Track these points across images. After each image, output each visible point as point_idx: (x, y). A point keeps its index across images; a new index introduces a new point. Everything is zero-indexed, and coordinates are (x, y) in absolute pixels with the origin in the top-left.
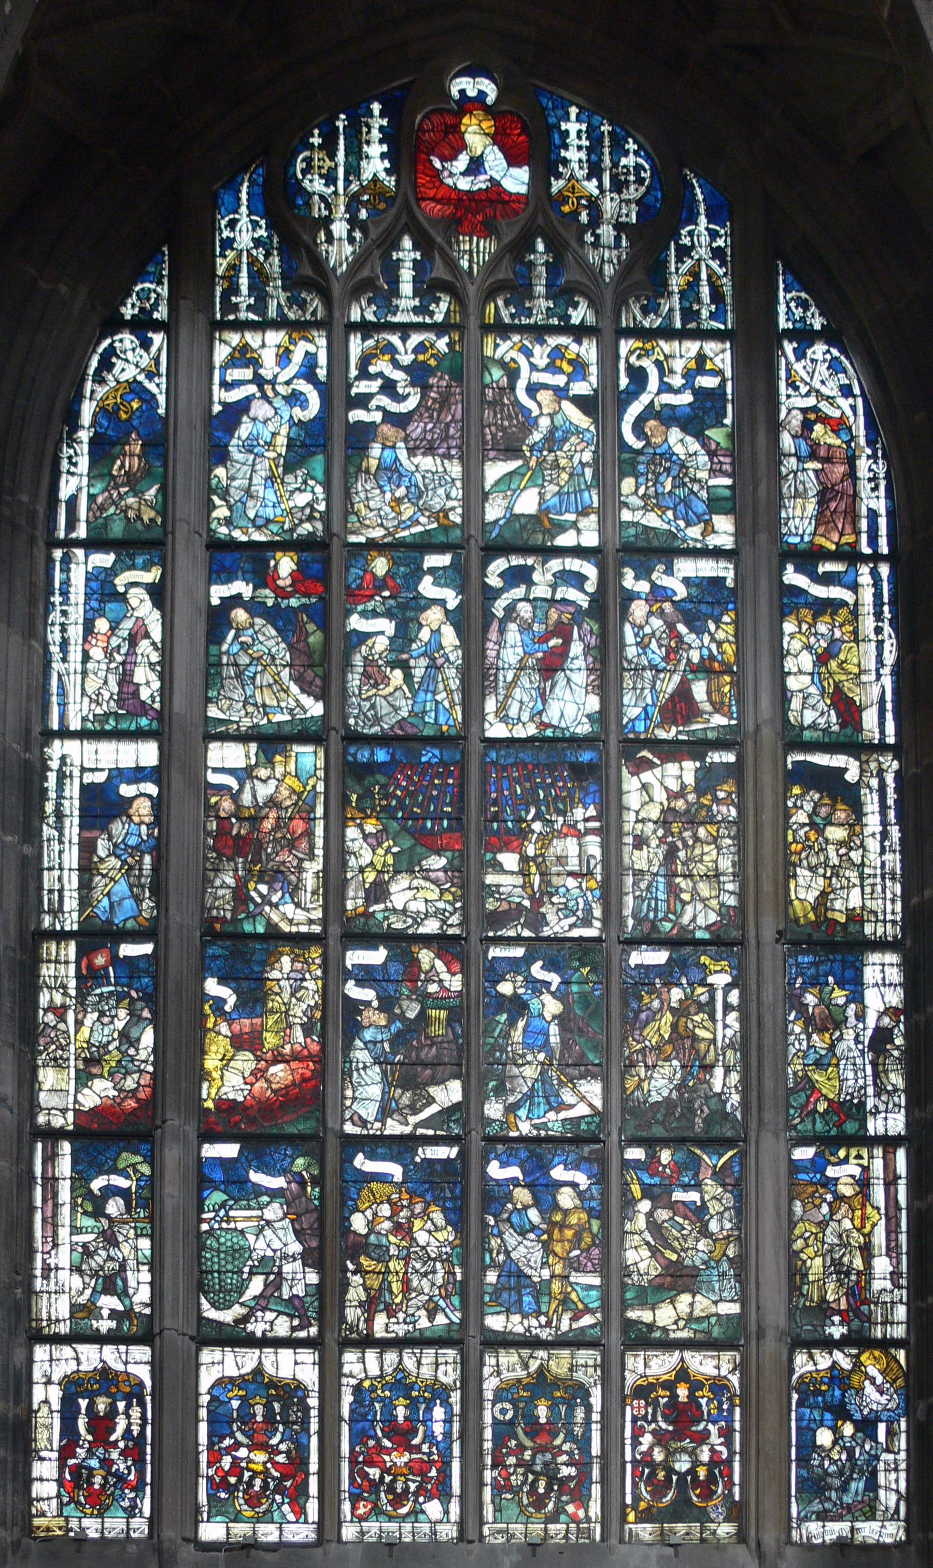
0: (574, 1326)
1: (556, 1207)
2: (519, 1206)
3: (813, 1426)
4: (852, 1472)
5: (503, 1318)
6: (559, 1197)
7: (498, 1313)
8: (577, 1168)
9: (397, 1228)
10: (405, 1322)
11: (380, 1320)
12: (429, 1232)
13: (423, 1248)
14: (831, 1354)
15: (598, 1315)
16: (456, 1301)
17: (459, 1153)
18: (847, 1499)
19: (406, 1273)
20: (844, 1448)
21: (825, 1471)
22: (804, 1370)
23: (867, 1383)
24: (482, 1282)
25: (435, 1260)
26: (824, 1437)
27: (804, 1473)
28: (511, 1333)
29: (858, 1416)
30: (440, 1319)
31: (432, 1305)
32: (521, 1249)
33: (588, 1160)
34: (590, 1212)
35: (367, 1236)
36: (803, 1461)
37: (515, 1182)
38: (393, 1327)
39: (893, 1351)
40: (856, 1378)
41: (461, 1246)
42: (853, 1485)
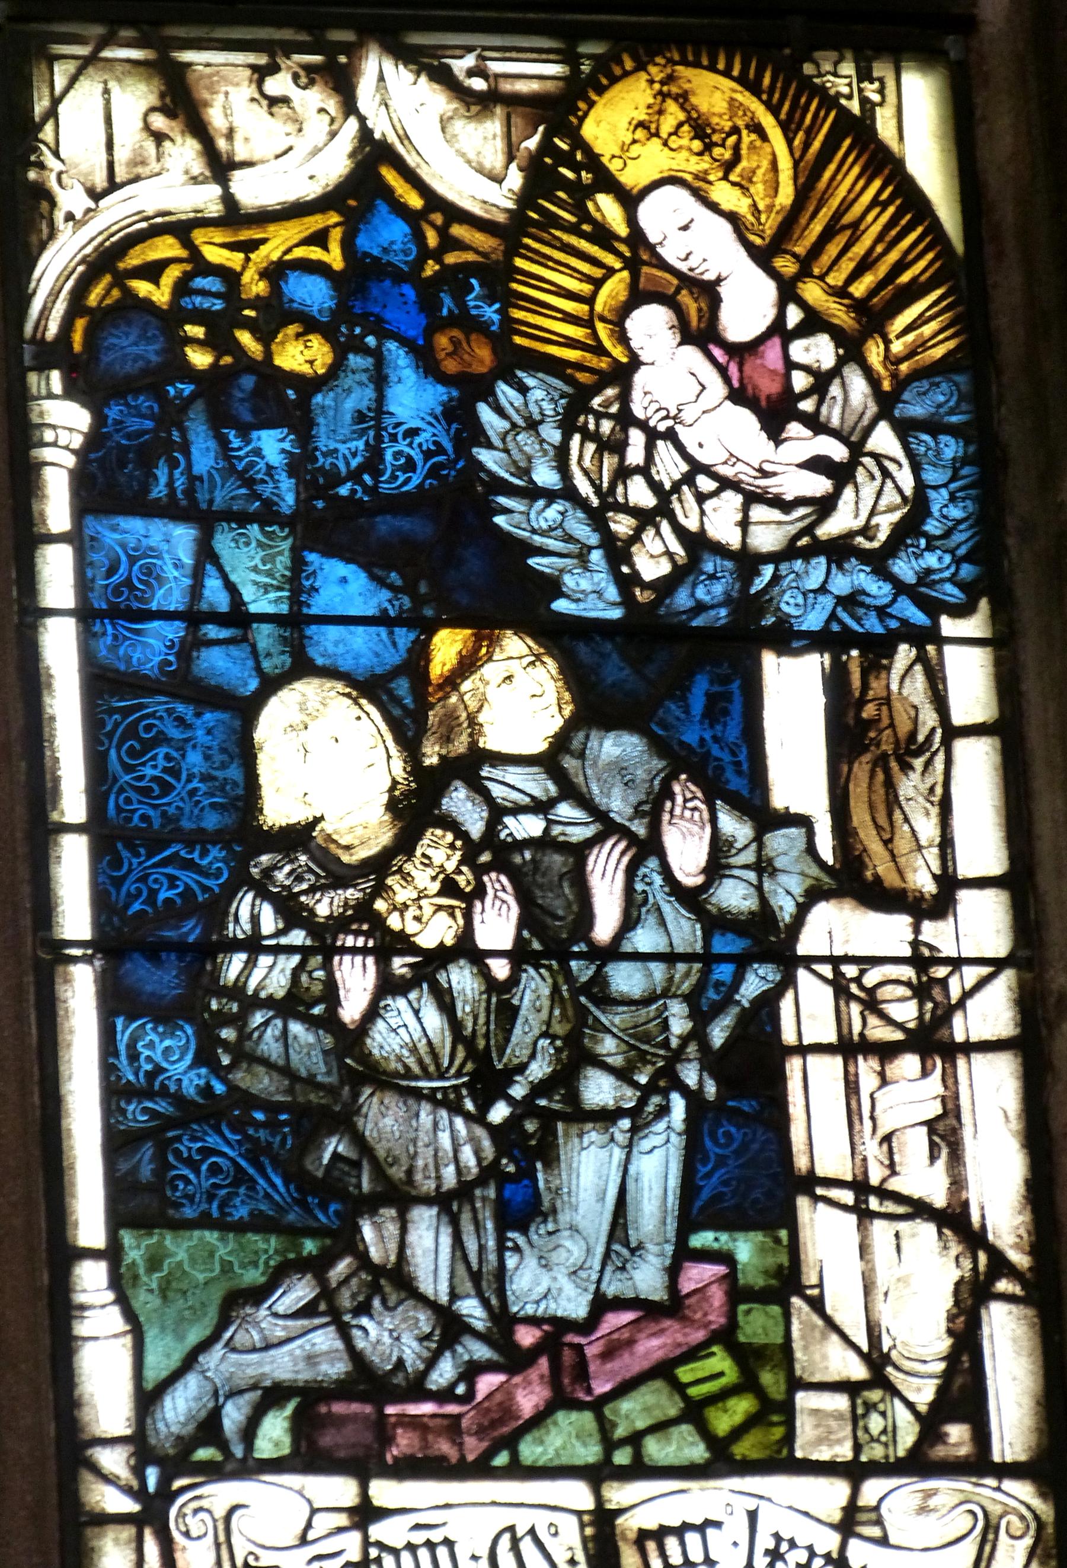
3: (221, 664)
4: (575, 1058)
14: (342, 84)
18: (549, 1282)
20: (490, 852)
21: (350, 1040)
22: (117, 212)
23: (650, 326)
26: (322, 762)
27: (170, 1053)
29: (589, 594)
36: (161, 953)
39: (841, 79)
40: (555, 286)
42: (588, 1168)
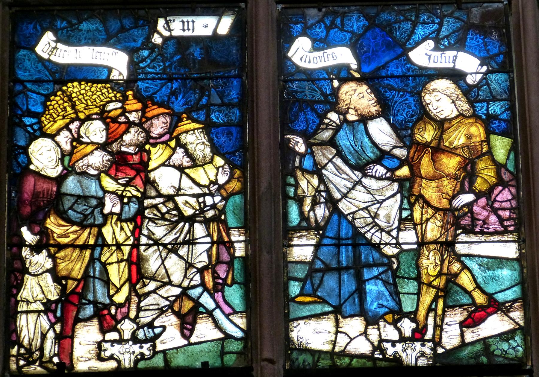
0: (470, 336)
1: (423, 115)
2: (352, 117)
5: (328, 324)
6: (427, 98)
7: (318, 316)
8: (460, 45)
9: (119, 161)
10: (135, 339)
11: (87, 335)
12: (181, 169)
13: (170, 198)
15: (517, 315)
16: (234, 295)
17: (234, 27)
19: (136, 245)
24: (283, 262)
25: (191, 220)
28: (343, 354)
30: (205, 330)
31: (188, 305)
32: (360, 196)
33: (482, 30)
34: (488, 122)
35: (60, 180)
37: (343, 74)
38: (110, 350)
41: (242, 192)
